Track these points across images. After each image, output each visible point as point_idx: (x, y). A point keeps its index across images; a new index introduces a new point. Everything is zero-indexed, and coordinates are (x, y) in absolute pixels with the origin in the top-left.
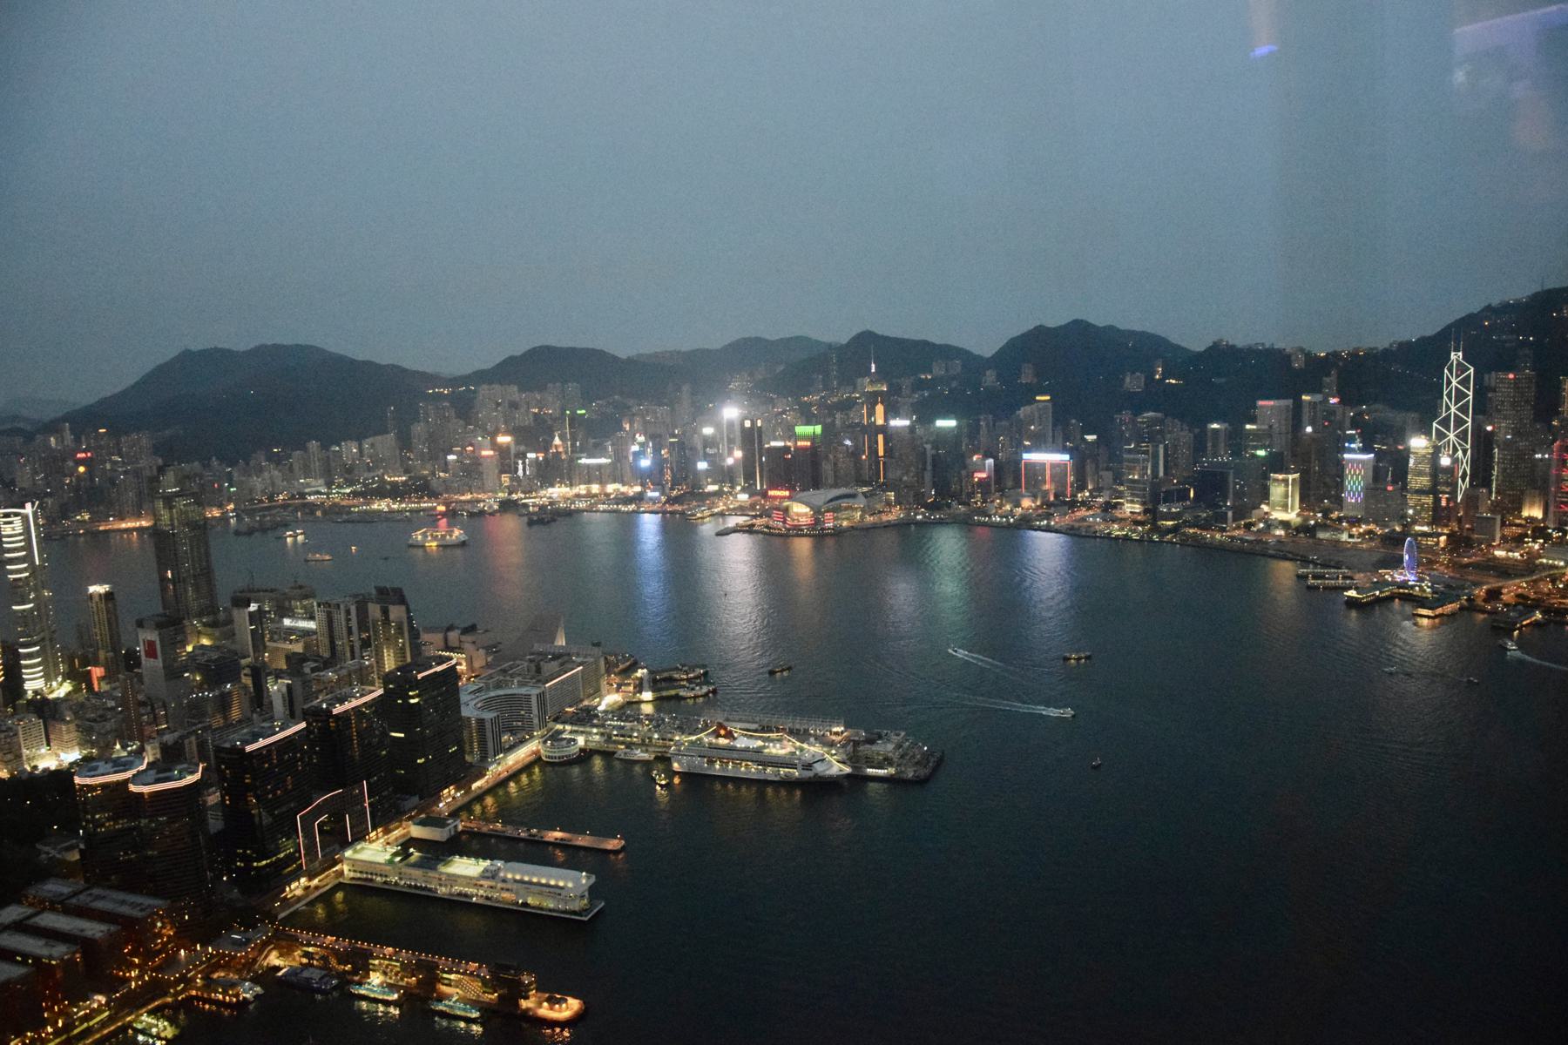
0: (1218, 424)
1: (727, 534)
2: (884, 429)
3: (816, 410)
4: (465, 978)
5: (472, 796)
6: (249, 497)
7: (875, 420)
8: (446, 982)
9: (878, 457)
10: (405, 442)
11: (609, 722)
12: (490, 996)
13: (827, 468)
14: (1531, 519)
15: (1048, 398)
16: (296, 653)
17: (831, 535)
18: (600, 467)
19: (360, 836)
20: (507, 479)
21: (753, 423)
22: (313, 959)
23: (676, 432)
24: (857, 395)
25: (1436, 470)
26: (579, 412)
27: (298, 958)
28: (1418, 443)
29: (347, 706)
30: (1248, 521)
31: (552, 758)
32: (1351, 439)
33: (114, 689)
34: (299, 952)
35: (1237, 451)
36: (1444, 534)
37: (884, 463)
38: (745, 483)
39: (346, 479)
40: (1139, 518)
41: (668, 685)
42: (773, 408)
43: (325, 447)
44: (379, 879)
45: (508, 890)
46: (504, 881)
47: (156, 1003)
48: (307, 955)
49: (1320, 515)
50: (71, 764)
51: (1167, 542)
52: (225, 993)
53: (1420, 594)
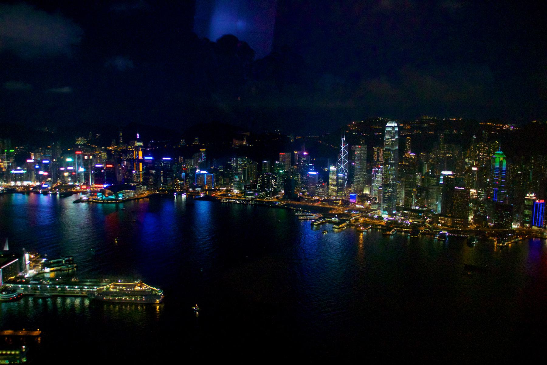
0: (266, 161)
1: (79, 202)
2: (142, 161)
7: (139, 157)
9: (139, 171)
11: (31, 282)
13: (120, 177)
14: (366, 194)
15: (205, 150)
21: (89, 157)
24: (130, 147)
25: (338, 179)
26: (11, 151)
28: (332, 168)
30: (277, 196)
31: (7, 299)
32: (311, 167)
35: (272, 170)
36: (340, 200)
37: (142, 174)
38: (85, 181)
40: (239, 195)
41: (58, 265)
42: (96, 151)
49: (301, 194)
51: (249, 204)
53: (334, 221)
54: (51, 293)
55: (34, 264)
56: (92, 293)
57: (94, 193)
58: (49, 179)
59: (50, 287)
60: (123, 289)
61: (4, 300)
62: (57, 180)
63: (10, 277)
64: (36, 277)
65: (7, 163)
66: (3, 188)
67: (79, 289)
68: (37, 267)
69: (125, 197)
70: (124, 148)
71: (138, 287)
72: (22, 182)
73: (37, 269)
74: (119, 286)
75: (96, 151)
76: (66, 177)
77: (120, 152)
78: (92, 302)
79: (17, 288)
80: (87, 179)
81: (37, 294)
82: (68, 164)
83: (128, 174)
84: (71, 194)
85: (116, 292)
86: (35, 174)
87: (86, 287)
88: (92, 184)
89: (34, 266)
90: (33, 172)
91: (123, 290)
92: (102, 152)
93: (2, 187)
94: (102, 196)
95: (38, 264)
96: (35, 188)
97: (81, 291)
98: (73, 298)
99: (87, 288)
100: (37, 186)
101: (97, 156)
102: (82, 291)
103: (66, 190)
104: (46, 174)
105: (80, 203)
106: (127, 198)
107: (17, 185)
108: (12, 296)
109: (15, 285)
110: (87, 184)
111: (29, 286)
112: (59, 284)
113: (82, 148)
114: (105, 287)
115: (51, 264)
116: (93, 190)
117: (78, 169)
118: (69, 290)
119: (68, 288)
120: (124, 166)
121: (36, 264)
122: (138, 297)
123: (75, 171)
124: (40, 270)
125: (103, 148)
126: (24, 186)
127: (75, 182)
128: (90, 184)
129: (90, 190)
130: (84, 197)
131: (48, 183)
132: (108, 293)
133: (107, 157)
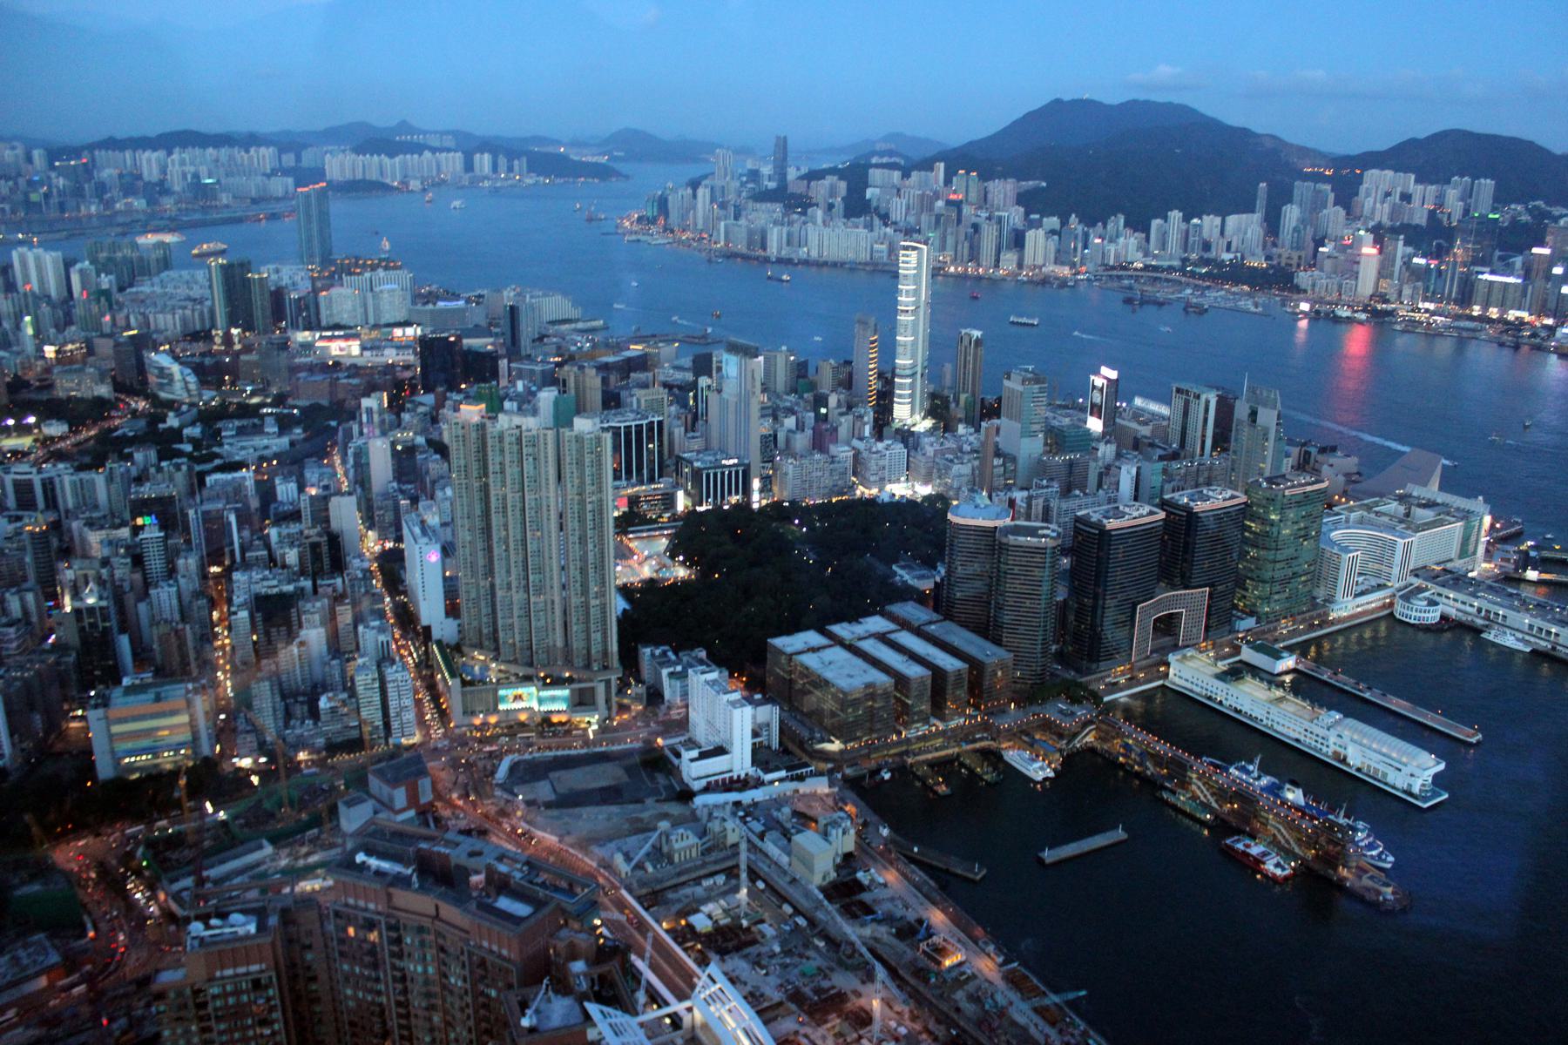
126: (1507, 323)
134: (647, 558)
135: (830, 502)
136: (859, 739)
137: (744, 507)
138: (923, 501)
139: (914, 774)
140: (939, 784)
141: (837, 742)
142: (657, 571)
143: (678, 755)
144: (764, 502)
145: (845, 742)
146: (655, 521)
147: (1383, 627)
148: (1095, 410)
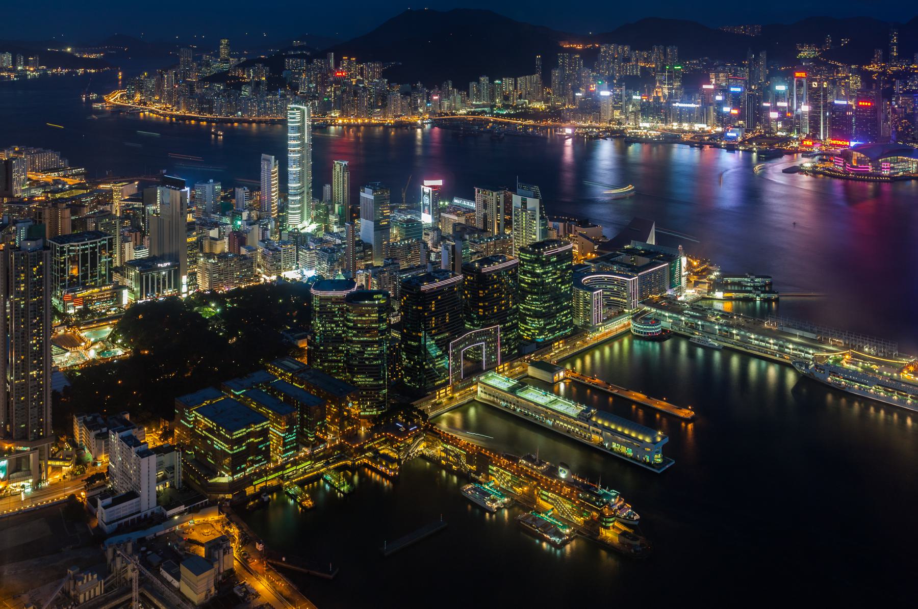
3: (876, 77)
4: (560, 498)
5: (576, 351)
6: (439, 111)
8: (545, 498)
10: (546, 81)
12: (577, 518)
16: (459, 224)
17: (887, 181)
18: (690, 110)
19: (492, 367)
20: (618, 114)
22: (450, 455)
23: (753, 87)
27: (439, 452)
29: (492, 268)
33: (341, 232)
34: (440, 447)
39: (503, 104)
42: (838, 73)
43: (491, 81)
44: (502, 403)
45: (597, 433)
46: (596, 425)
47: (341, 463)
48: (446, 451)
50: (309, 279)
52: (387, 466)
54: (720, 341)
55: (695, 277)
56: (804, 363)
57: (826, 156)
58: (741, 122)
59: (719, 330)
60: (872, 369)
61: (637, 334)
62: (755, 126)
63: (651, 293)
64: (700, 303)
65: (669, 89)
66: (659, 133)
67: (776, 347)
68: (700, 285)
69: (896, 171)
70: (901, 67)
71: (909, 372)
72: (692, 125)
73: (699, 289)
74: (865, 359)
75: (838, 72)
76: (772, 120)
77: (891, 76)
78: (803, 379)
79: (662, 318)
80: (815, 128)
81: (695, 338)
82: (778, 97)
83: (905, 122)
84: (779, 154)
85: (855, 373)
86: (715, 110)
87: (791, 346)
88: (825, 139)
89: (696, 284)
90: (712, 108)
91: (872, 370)
92: (852, 76)
93: (657, 131)
94: (844, 163)
95: (703, 281)
96: (713, 137)
97: (779, 351)
98: (764, 363)
99: (793, 349)
100: (717, 133)
101: (840, 83)
102: (781, 351)
103: (771, 145)
104: (735, 112)
105: (797, 174)
106: (901, 173)
107: (683, 129)
108: (647, 329)
109: (658, 311)
110: (813, 137)
111: (683, 318)
112: (738, 327)
113: (809, 67)
114: (832, 356)
115: (727, 284)
116: (826, 150)
117: (798, 107)
118: (756, 345)
119: (755, 339)
120: (896, 106)
121: (699, 279)
122: (907, 396)
123: (791, 110)
124: (706, 291)
125: (853, 67)
126: (694, 132)
127: (790, 131)
128: (822, 138)
129: (820, 150)
130: (807, 163)
131: (738, 129)
132: (835, 370)
133: (862, 86)
134: (93, 344)
135: (239, 288)
136: (244, 469)
137: (172, 300)
138: (308, 282)
139: (287, 493)
140: (306, 499)
141: (227, 475)
142: (99, 354)
143: (96, 506)
144: (191, 292)
145: (232, 476)
146: (105, 314)
147: (626, 341)
148: (426, 208)
